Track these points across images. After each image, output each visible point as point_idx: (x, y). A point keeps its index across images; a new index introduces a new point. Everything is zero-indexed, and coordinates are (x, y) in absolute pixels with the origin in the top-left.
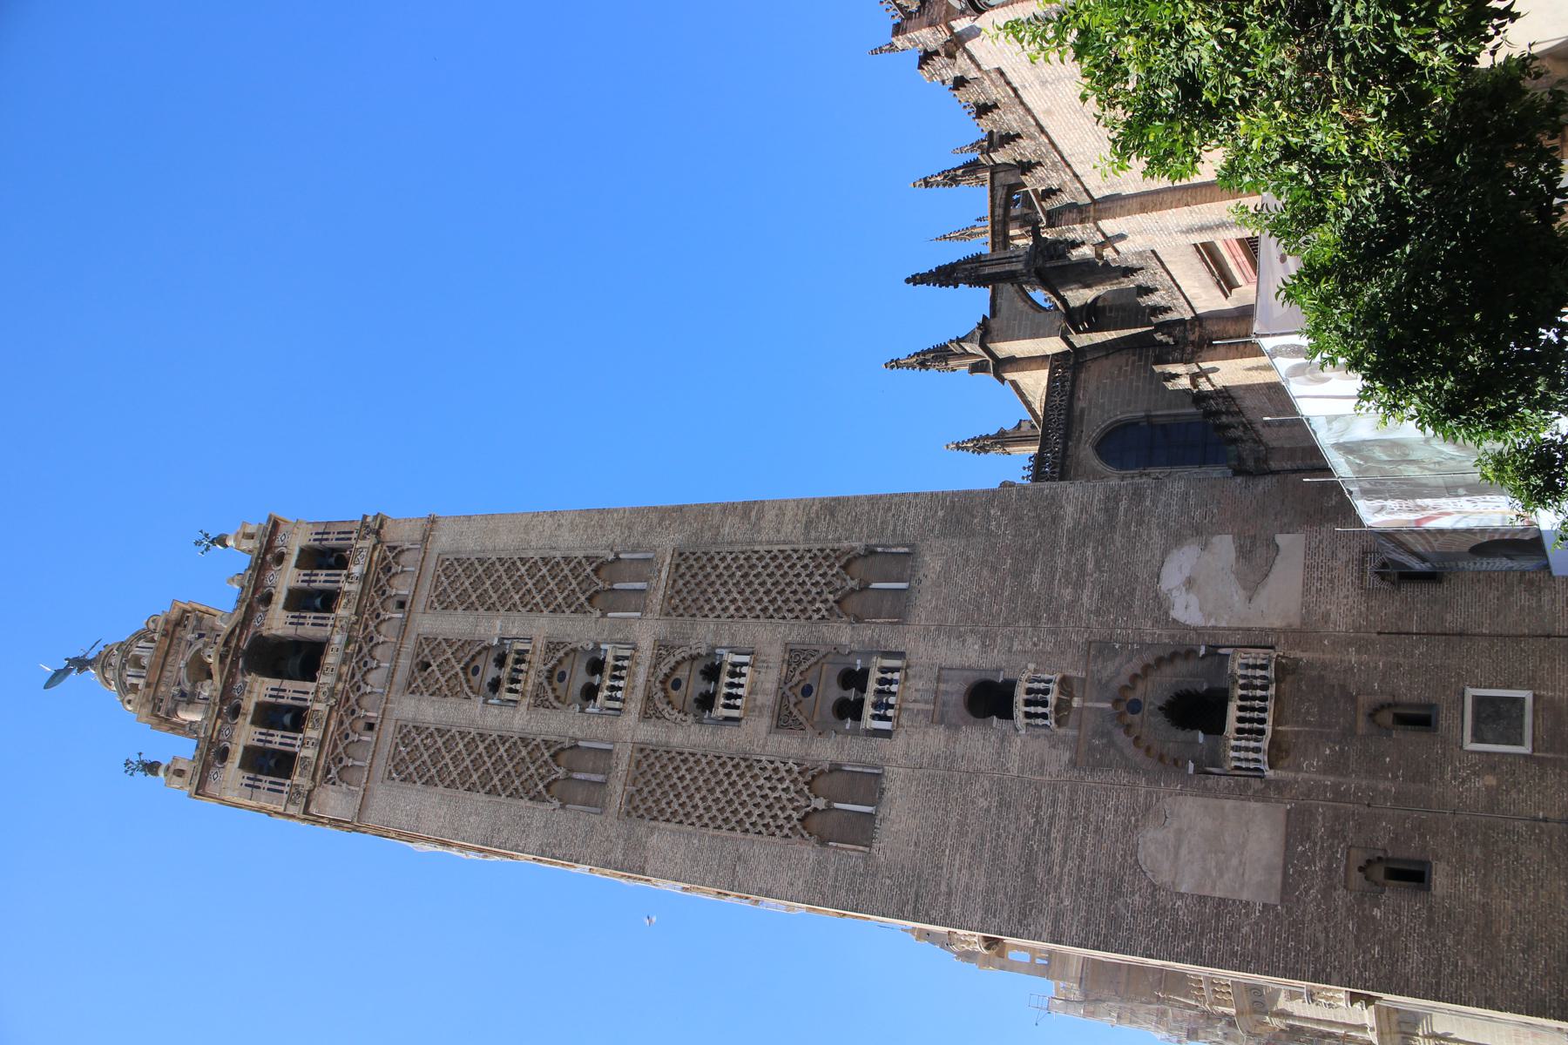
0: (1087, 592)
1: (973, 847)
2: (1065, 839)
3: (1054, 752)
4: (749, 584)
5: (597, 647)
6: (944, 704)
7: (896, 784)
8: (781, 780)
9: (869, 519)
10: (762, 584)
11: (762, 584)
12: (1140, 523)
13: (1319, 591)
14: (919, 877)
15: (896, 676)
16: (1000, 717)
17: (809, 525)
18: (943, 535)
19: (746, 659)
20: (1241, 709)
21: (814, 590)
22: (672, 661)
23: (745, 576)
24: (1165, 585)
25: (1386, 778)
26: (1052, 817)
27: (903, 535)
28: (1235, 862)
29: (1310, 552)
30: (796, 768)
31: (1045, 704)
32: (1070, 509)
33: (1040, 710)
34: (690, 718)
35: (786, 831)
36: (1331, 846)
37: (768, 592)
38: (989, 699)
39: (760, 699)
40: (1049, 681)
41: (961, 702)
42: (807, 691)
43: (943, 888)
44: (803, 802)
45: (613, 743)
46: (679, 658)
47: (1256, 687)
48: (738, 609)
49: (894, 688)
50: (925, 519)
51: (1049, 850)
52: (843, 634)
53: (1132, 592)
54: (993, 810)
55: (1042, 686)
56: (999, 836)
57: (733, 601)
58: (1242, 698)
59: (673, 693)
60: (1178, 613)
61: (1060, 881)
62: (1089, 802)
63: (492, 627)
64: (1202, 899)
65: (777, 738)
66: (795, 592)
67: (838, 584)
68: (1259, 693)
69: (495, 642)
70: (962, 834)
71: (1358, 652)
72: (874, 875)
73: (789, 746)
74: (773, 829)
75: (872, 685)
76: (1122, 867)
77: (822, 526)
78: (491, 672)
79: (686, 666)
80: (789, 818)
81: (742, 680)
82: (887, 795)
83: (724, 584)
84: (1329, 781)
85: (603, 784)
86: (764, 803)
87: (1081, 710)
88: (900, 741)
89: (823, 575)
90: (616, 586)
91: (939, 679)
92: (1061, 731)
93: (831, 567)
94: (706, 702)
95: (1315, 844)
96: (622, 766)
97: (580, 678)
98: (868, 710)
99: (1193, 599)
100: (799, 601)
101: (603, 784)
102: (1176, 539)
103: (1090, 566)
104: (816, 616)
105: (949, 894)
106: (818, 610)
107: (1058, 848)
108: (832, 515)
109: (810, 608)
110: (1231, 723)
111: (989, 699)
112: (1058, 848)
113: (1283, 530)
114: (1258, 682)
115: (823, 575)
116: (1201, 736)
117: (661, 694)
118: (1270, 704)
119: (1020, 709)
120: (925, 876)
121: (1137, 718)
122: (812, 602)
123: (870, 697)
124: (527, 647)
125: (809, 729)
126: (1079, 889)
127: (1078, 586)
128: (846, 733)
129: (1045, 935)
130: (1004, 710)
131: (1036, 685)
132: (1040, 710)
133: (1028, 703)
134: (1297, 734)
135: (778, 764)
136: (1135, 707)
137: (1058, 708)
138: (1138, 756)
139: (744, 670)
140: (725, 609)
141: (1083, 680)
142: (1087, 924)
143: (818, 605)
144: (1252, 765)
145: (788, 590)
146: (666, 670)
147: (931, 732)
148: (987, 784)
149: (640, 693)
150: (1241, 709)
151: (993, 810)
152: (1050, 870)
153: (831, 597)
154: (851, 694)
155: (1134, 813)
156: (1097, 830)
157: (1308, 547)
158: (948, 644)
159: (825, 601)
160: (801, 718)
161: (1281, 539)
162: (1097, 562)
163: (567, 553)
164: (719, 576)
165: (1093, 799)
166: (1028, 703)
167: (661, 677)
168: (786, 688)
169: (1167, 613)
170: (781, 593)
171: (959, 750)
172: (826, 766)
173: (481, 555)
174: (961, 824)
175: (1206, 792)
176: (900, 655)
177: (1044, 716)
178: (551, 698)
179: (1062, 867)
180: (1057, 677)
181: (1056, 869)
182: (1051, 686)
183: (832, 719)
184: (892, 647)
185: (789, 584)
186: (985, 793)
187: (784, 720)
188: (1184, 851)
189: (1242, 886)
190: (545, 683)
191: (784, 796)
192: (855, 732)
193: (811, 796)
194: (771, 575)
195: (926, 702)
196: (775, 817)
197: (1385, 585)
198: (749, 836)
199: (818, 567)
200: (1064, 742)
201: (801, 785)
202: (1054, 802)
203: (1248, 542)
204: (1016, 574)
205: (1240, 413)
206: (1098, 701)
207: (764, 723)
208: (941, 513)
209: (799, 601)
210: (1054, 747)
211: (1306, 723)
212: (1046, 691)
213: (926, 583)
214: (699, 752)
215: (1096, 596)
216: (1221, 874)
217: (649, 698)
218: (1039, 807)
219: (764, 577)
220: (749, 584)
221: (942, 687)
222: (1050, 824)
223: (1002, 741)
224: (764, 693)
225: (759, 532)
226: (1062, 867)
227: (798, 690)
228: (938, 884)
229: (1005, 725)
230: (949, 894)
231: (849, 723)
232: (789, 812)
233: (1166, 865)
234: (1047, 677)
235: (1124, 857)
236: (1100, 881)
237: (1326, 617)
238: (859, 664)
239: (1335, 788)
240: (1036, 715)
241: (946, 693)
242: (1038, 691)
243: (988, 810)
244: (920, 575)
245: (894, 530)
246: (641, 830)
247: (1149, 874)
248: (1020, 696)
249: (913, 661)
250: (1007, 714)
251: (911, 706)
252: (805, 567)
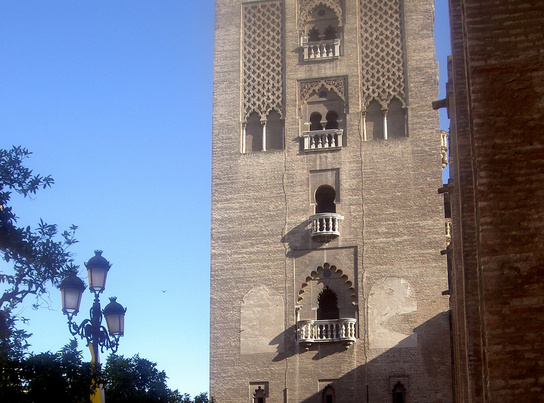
1: (250, 207)
2: (258, 252)
3: (300, 238)
4: (382, 42)
7: (277, 158)
8: (273, 94)
9: (423, 106)
10: (382, 50)
11: (382, 50)
12: (423, 262)
14: (232, 183)
15: (333, 145)
17: (418, 69)
18: (413, 152)
19: (337, 54)
21: (380, 83)
23: (387, 37)
27: (415, 129)
28: (257, 333)
31: (321, 229)
32: (430, 222)
37: (377, 55)
38: (326, 199)
40: (334, 229)
41: (324, 183)
43: (230, 196)
44: (264, 109)
48: (367, 39)
49: (327, 146)
50: (424, 140)
51: (252, 245)
52: (357, 105)
55: (331, 226)
57: (371, 35)
58: (332, 326)
61: (239, 254)
62: (277, 260)
64: (239, 321)
66: (378, 72)
67: (384, 96)
68: (335, 333)
70: (256, 199)
72: (231, 159)
76: (249, 281)
77: (420, 78)
80: (254, 104)
81: (325, 55)
83: (381, 26)
84: (297, 370)
86: (260, 88)
89: (389, 87)
92: (311, 240)
93: (394, 90)
100: (373, 76)
103: (397, 239)
104: (364, 89)
105: (227, 200)
106: (368, 89)
107: (255, 249)
108: (425, 82)
109: (369, 84)
112: (255, 249)
115: (389, 87)
116: (315, 309)
120: (234, 186)
122: (373, 84)
126: (236, 263)
127: (386, 234)
129: (214, 251)
131: (331, 222)
139: (331, 55)
140: (366, 31)
142: (221, 270)
143: (371, 88)
145: (379, 67)
147: (305, 171)
148: (281, 207)
152: (243, 247)
153: (376, 95)
154: (324, 121)
155: (274, 283)
156: (264, 267)
157: (411, 349)
158: (353, 170)
159: (374, 92)
162: (400, 242)
164: (386, 21)
170: (378, 64)
171: (298, 189)
174: (261, 199)
176: (344, 144)
179: (245, 253)
180: (337, 233)
181: (244, 250)
182: (331, 230)
184: (349, 138)
185: (383, 67)
186: (277, 207)
188: (259, 309)
189: (246, 338)
191: (265, 98)
194: (388, 54)
195: (320, 165)
196: (254, 96)
197: (392, 387)
199: (394, 82)
201: (272, 106)
204: (392, 199)
208: (427, 149)
209: (373, 76)
212: (328, 229)
213: (386, 150)
216: (250, 327)
219: (386, 50)
220: (382, 42)
222: (265, 243)
224: (319, 69)
225: (414, 38)
226: (245, 253)
228: (231, 193)
230: (227, 200)
231: (308, 124)
232: (257, 103)
233: (252, 302)
234: (336, 226)
235: (254, 282)
236: (241, 272)
238: (339, 121)
242: (328, 225)
243: (270, 211)
244: (391, 145)
245: (416, 123)
247: (247, 295)
249: (343, 151)
252: (394, 74)
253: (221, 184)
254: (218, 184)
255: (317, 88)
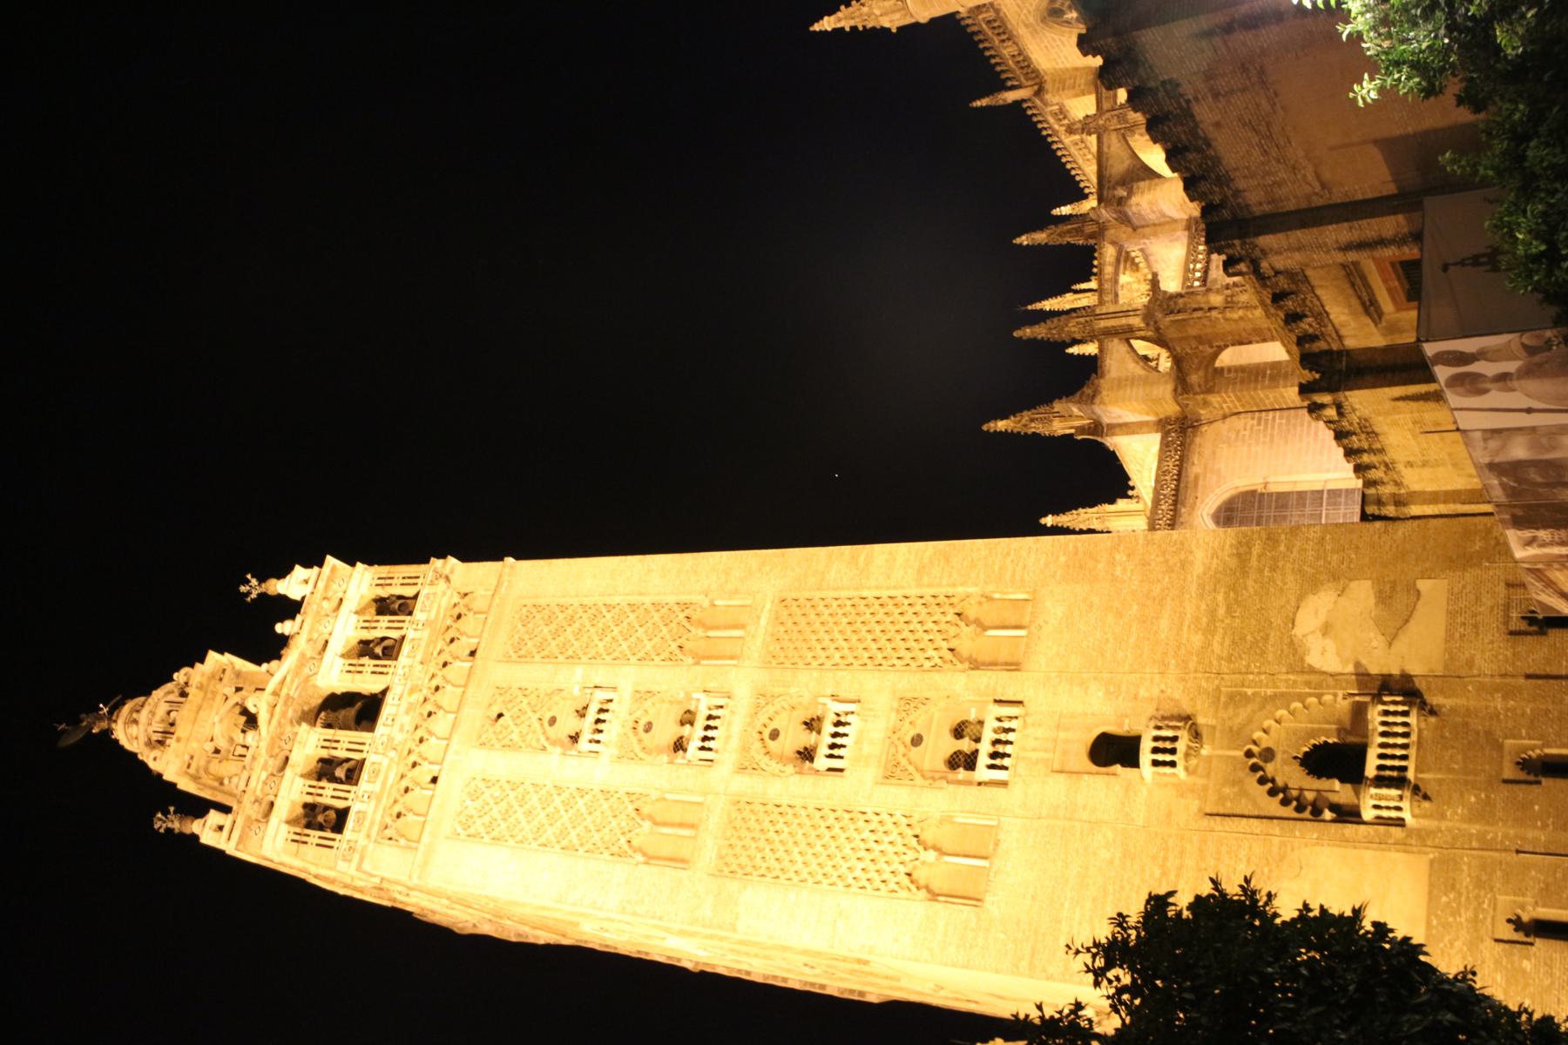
0: (1217, 638)
1: (1094, 899)
5: (688, 698)
6: (1065, 753)
13: (1462, 636)
16: (1123, 765)
20: (1381, 756)
22: (771, 710)
24: (1298, 631)
25: (1535, 827)
26: (1180, 868)
29: (1453, 596)
30: (905, 821)
31: (1173, 751)
33: (1168, 758)
34: (790, 769)
35: (892, 886)
36: (1477, 897)
38: (1114, 751)
39: (866, 749)
42: (917, 741)
45: (705, 794)
46: (777, 707)
47: (1396, 735)
53: (1266, 638)
54: (1117, 862)
55: (1170, 733)
56: (1122, 888)
58: (1382, 745)
59: (772, 745)
60: (1313, 660)
63: (574, 679)
65: (885, 788)
68: (1400, 741)
69: (576, 692)
71: (1504, 698)
73: (898, 798)
74: (877, 883)
75: (988, 735)
78: (568, 724)
79: (785, 715)
82: (1003, 846)
84: (1474, 829)
85: (694, 838)
86: (869, 856)
87: (1209, 759)
88: (1016, 790)
90: (711, 633)
91: (1058, 727)
94: (807, 755)
95: (1460, 894)
96: (714, 820)
97: (667, 730)
98: (983, 760)
99: (1330, 644)
101: (694, 838)
102: (1312, 584)
110: (1370, 771)
111: (1114, 751)
113: (1425, 575)
114: (1400, 730)
117: (758, 745)
118: (1412, 752)
119: (1146, 757)
121: (1270, 769)
123: (985, 748)
124: (609, 695)
125: (919, 780)
128: (959, 782)
130: (1132, 760)
132: (1168, 758)
133: (1155, 750)
134: (1440, 782)
135: (884, 816)
136: (1268, 754)
137: (1187, 755)
138: (1273, 806)
139: (849, 719)
141: (1214, 728)
144: (1394, 814)
146: (763, 718)
148: (1110, 835)
149: (735, 743)
150: (1381, 756)
151: (1117, 862)
160: (911, 769)
161: (1423, 585)
163: (657, 599)
165: (1224, 849)
166: (1155, 750)
167: (759, 727)
168: (895, 737)
169: (1302, 660)
172: (938, 815)
173: (562, 601)
175: (1345, 841)
177: (1173, 764)
178: (637, 748)
183: (943, 767)
187: (892, 773)
190: (630, 733)
191: (890, 849)
192: (968, 783)
193: (920, 848)
195: (1046, 751)
198: (852, 889)
200: (1193, 791)
202: (1182, 852)
203: (1387, 588)
205: (1382, 451)
206: (1229, 748)
207: (871, 773)
210: (1182, 796)
211: (1450, 770)
212: (1174, 739)
214: (798, 802)
215: (1227, 642)
217: (745, 749)
218: (1165, 858)
221: (1062, 735)
223: (1127, 790)
227: (908, 740)
229: (1128, 772)
231: (962, 773)
237: (1470, 663)
239: (1481, 837)
240: (1164, 764)
241: (1067, 741)
242: (1165, 739)
243: (1111, 862)
246: (733, 886)
248: (1146, 745)
250: (1132, 760)
251: (1029, 754)
253: (1033, 955)
254: (1031, 962)
255: (902, 749)
